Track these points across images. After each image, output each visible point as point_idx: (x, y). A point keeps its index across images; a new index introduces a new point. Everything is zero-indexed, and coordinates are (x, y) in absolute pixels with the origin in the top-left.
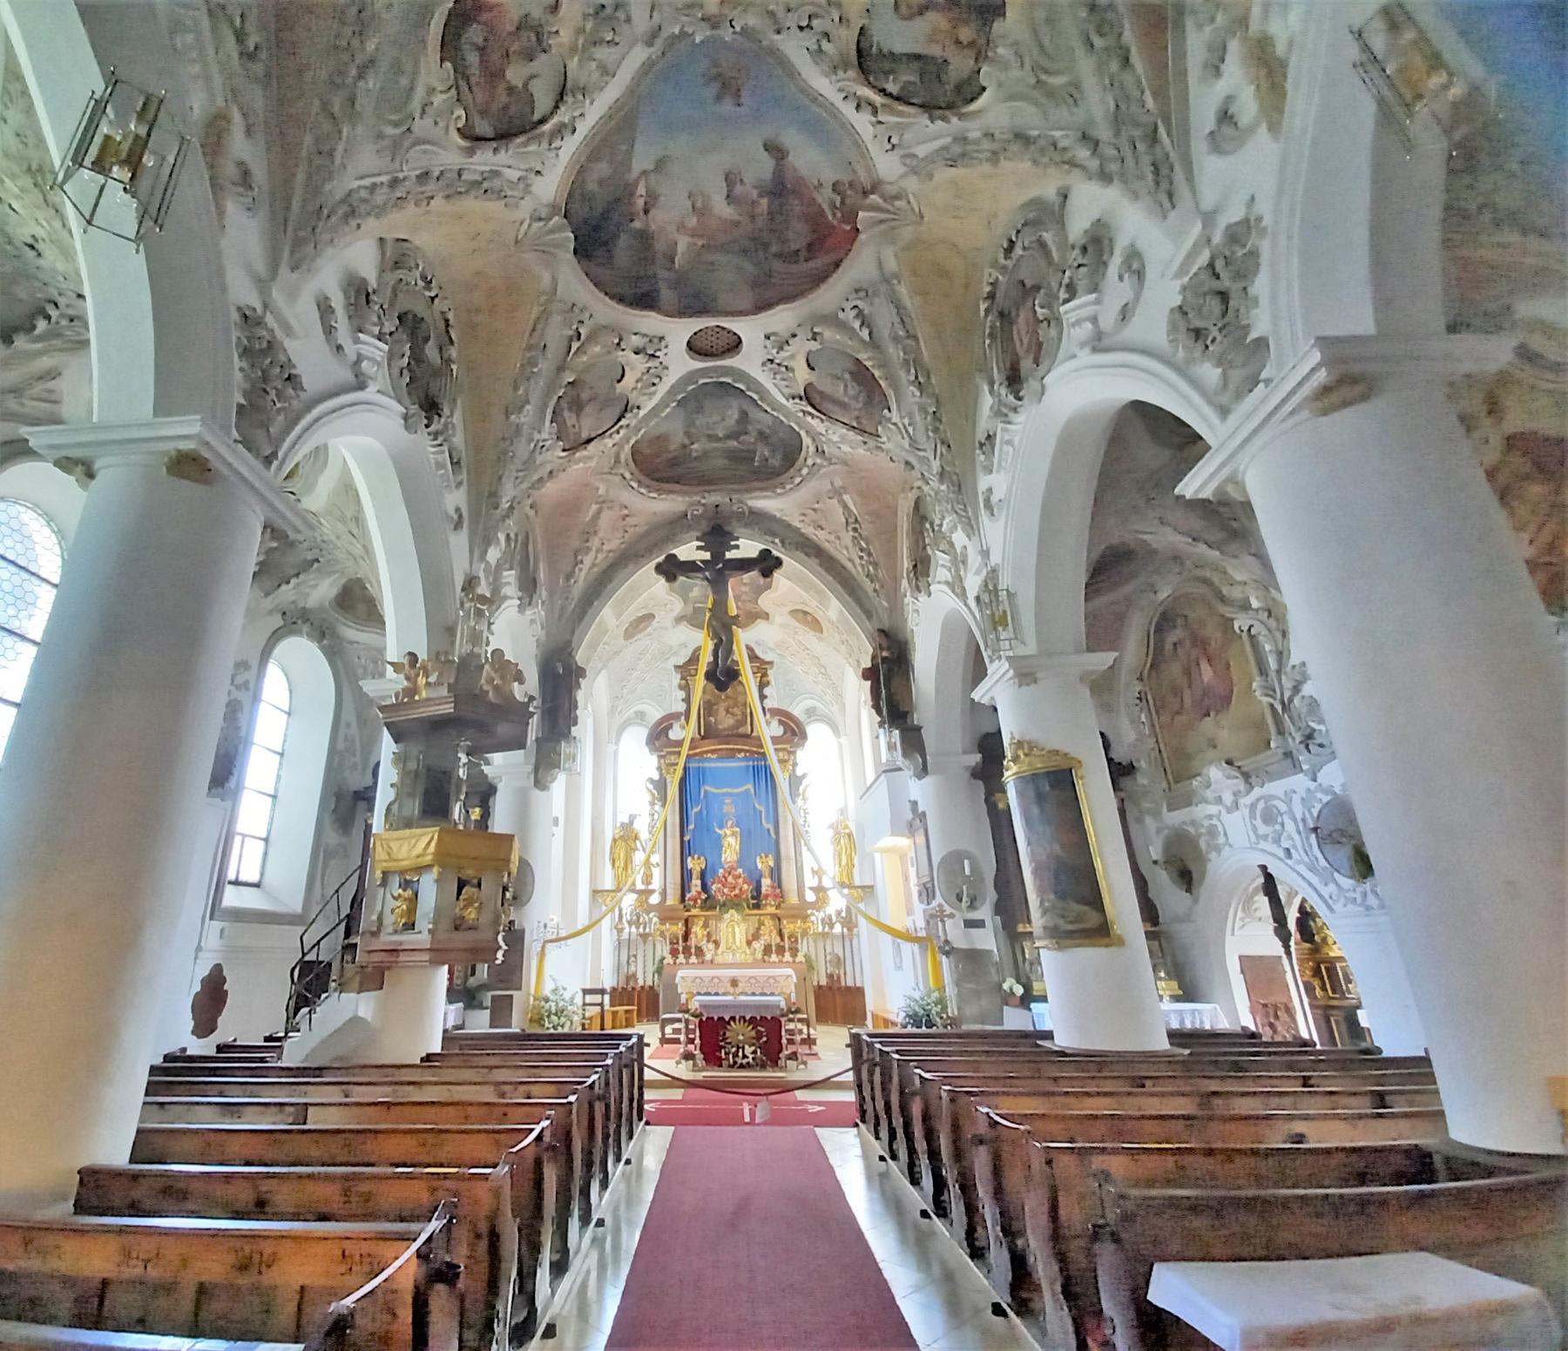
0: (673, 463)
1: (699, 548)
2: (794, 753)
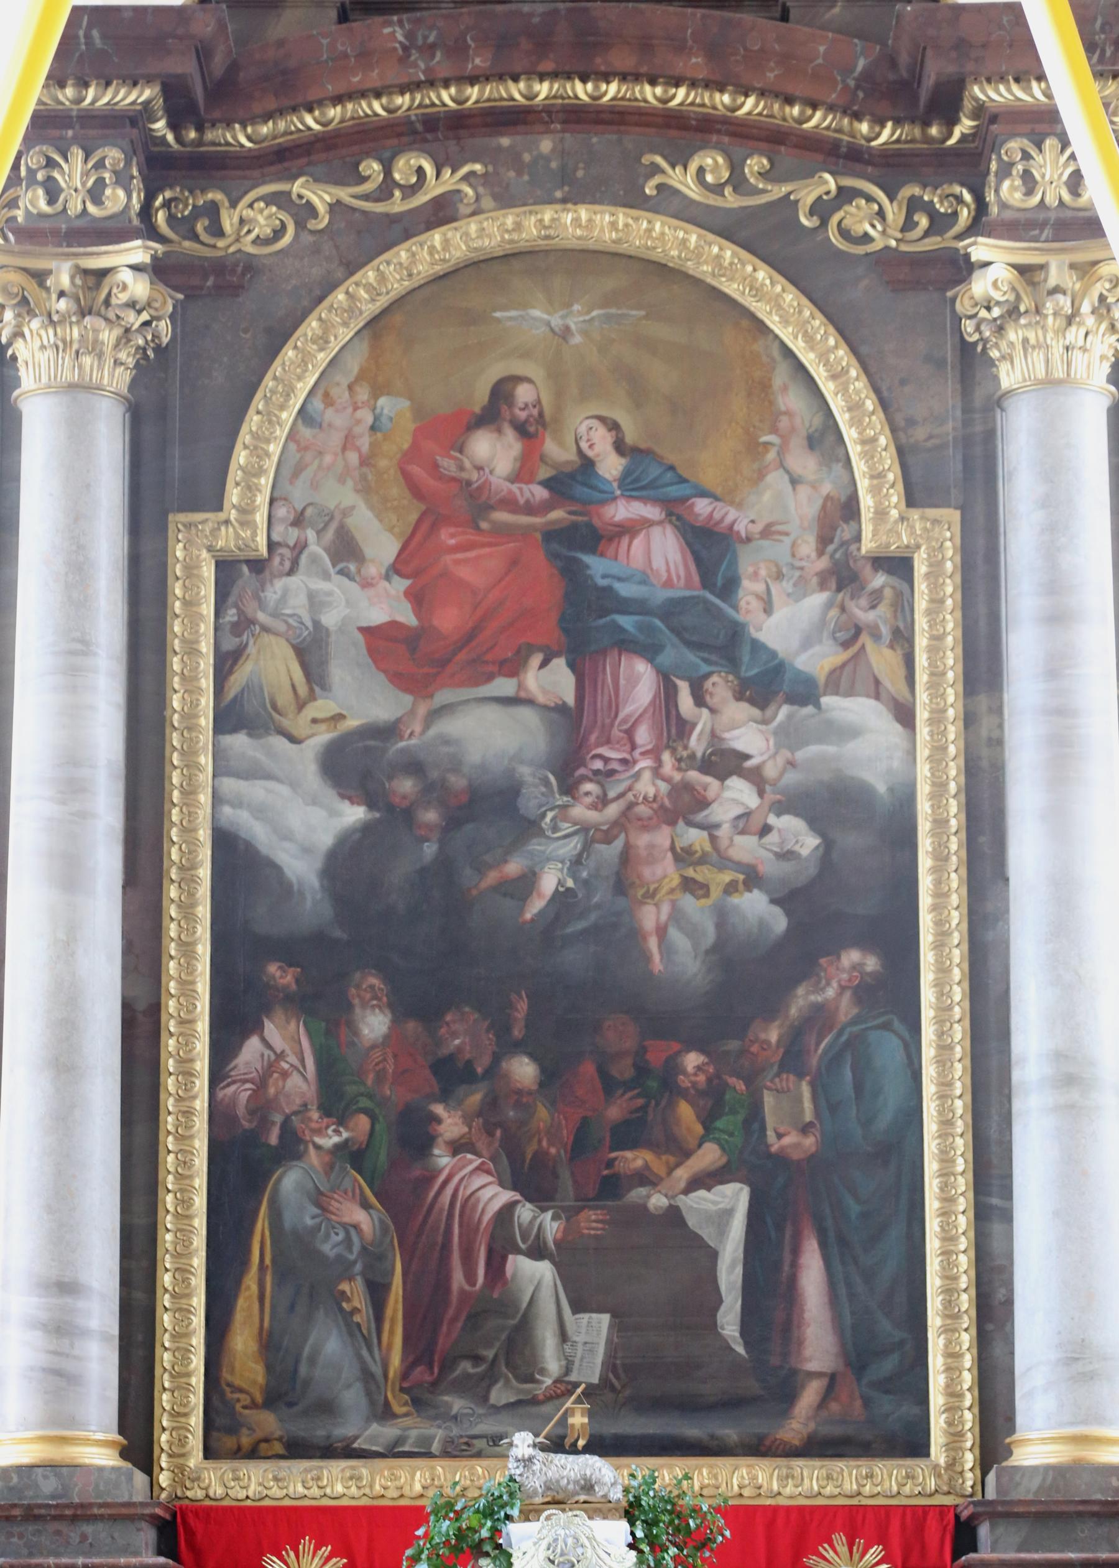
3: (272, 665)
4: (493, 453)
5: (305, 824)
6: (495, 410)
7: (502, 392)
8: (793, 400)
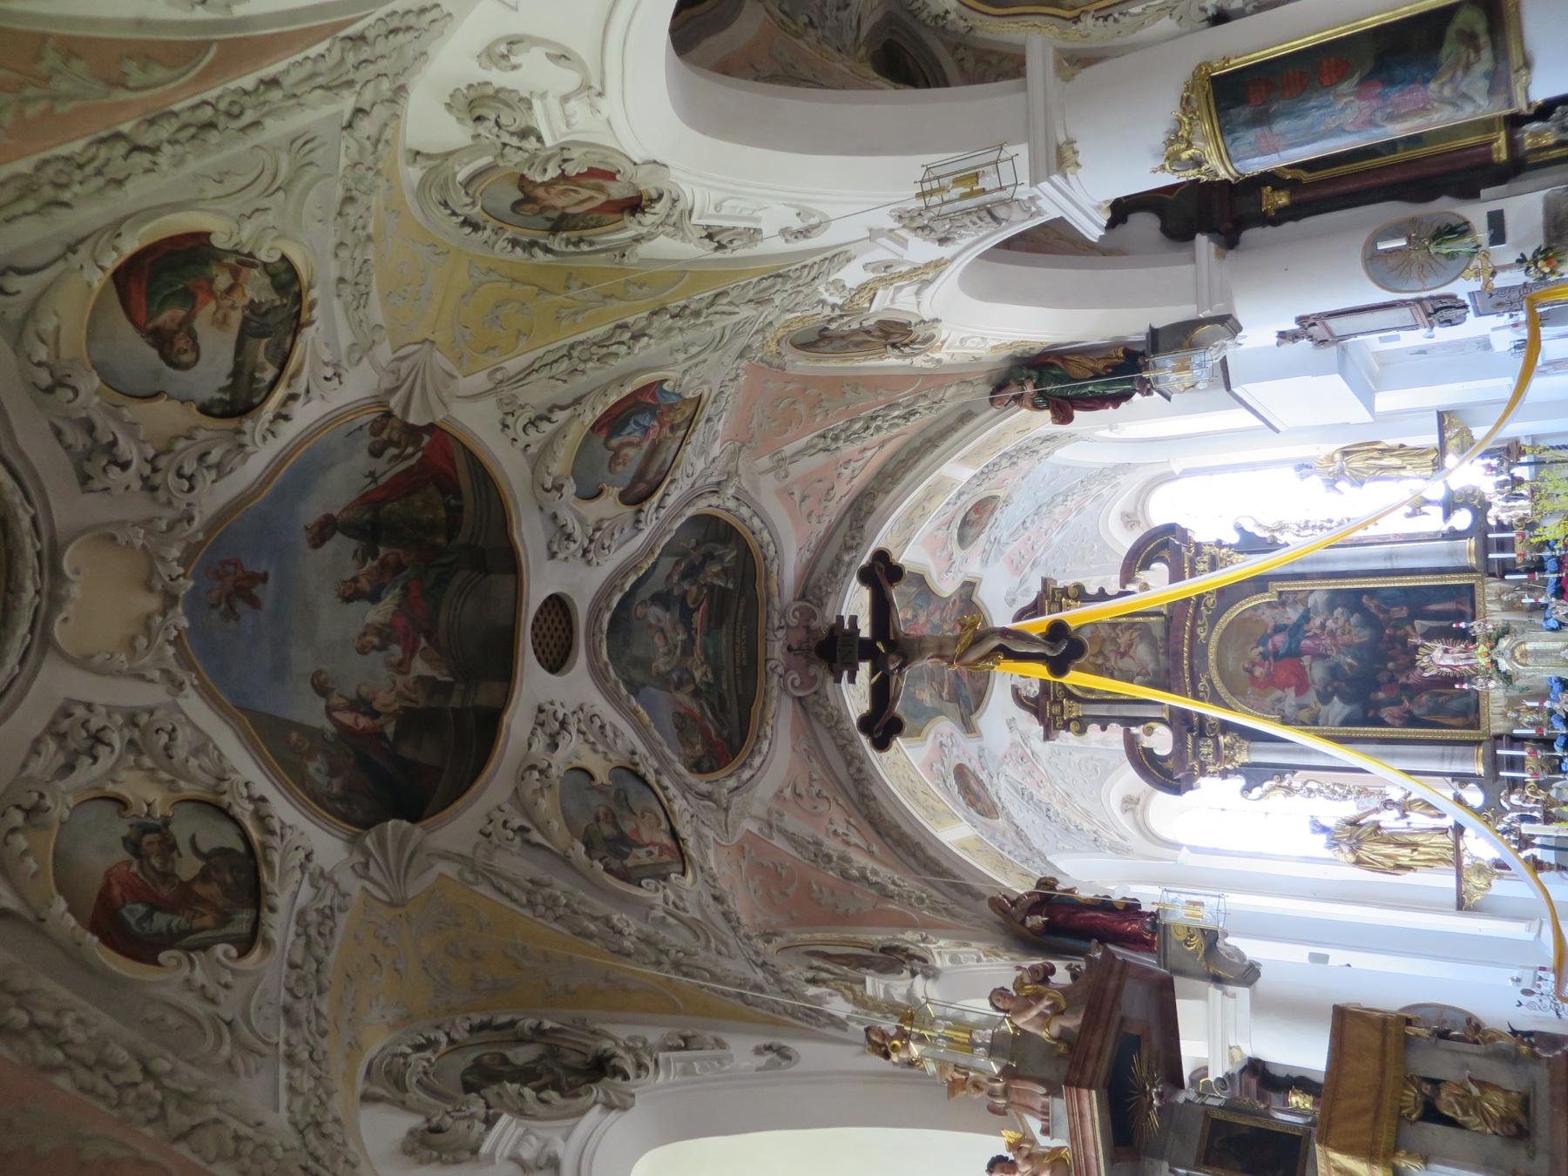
0: (720, 708)
1: (852, 680)
2: (1198, 546)
3: (1304, 715)
4: (1258, 672)
5: (1338, 708)
6: (1250, 671)
7: (1246, 670)
8: (1247, 615)
